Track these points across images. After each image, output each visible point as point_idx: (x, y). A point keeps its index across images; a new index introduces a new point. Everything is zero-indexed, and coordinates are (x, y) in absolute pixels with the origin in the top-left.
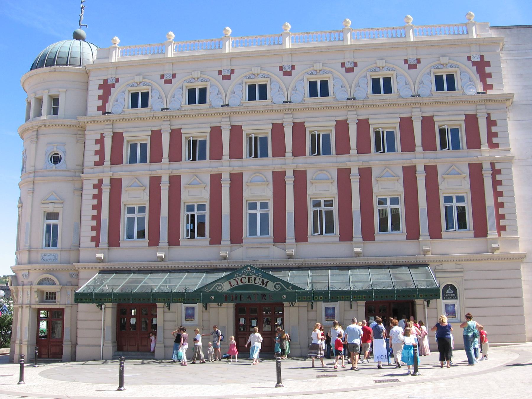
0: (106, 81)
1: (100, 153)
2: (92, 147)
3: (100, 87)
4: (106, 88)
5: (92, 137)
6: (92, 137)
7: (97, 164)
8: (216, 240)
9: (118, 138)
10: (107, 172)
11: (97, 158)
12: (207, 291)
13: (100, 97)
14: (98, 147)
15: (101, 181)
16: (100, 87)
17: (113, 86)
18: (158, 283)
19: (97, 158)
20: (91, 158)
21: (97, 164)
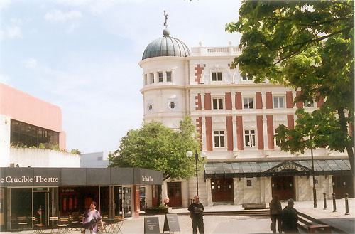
0: (198, 65)
1: (199, 103)
2: (193, 101)
3: (195, 69)
4: (199, 70)
5: (194, 94)
6: (194, 94)
7: (197, 109)
8: (261, 147)
9: (208, 96)
10: (204, 113)
11: (197, 106)
12: (271, 171)
13: (196, 74)
14: (197, 101)
15: (200, 118)
16: (195, 69)
17: (203, 69)
18: (236, 169)
19: (197, 106)
20: (194, 106)
21: (197, 109)
